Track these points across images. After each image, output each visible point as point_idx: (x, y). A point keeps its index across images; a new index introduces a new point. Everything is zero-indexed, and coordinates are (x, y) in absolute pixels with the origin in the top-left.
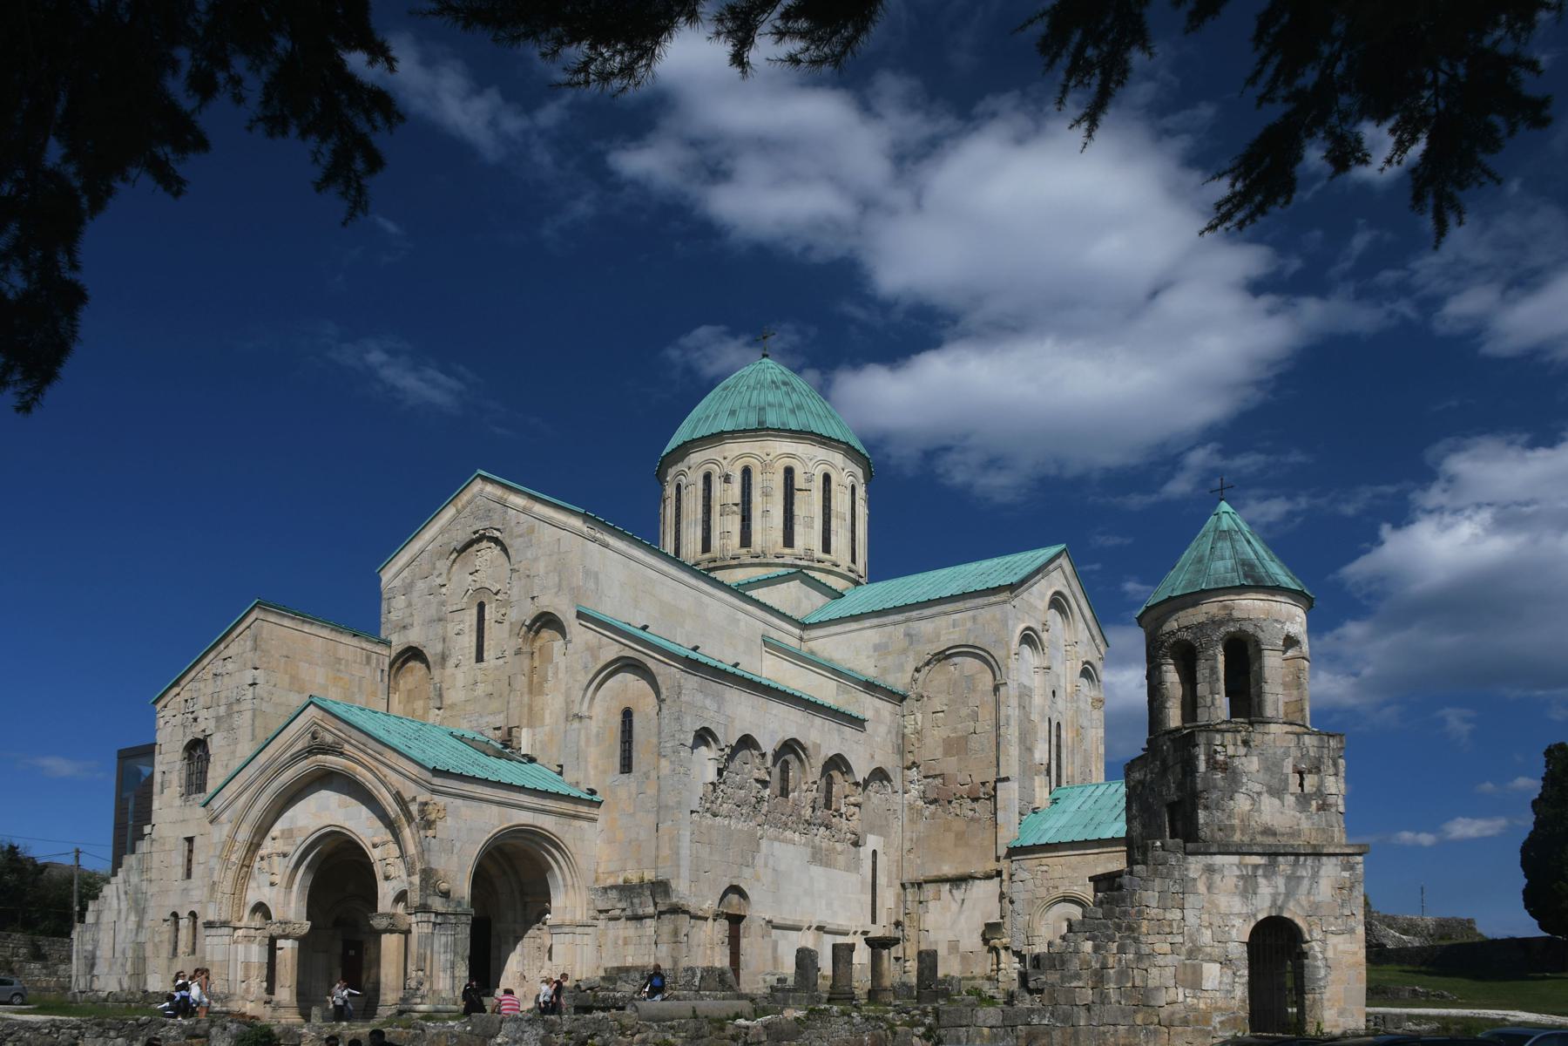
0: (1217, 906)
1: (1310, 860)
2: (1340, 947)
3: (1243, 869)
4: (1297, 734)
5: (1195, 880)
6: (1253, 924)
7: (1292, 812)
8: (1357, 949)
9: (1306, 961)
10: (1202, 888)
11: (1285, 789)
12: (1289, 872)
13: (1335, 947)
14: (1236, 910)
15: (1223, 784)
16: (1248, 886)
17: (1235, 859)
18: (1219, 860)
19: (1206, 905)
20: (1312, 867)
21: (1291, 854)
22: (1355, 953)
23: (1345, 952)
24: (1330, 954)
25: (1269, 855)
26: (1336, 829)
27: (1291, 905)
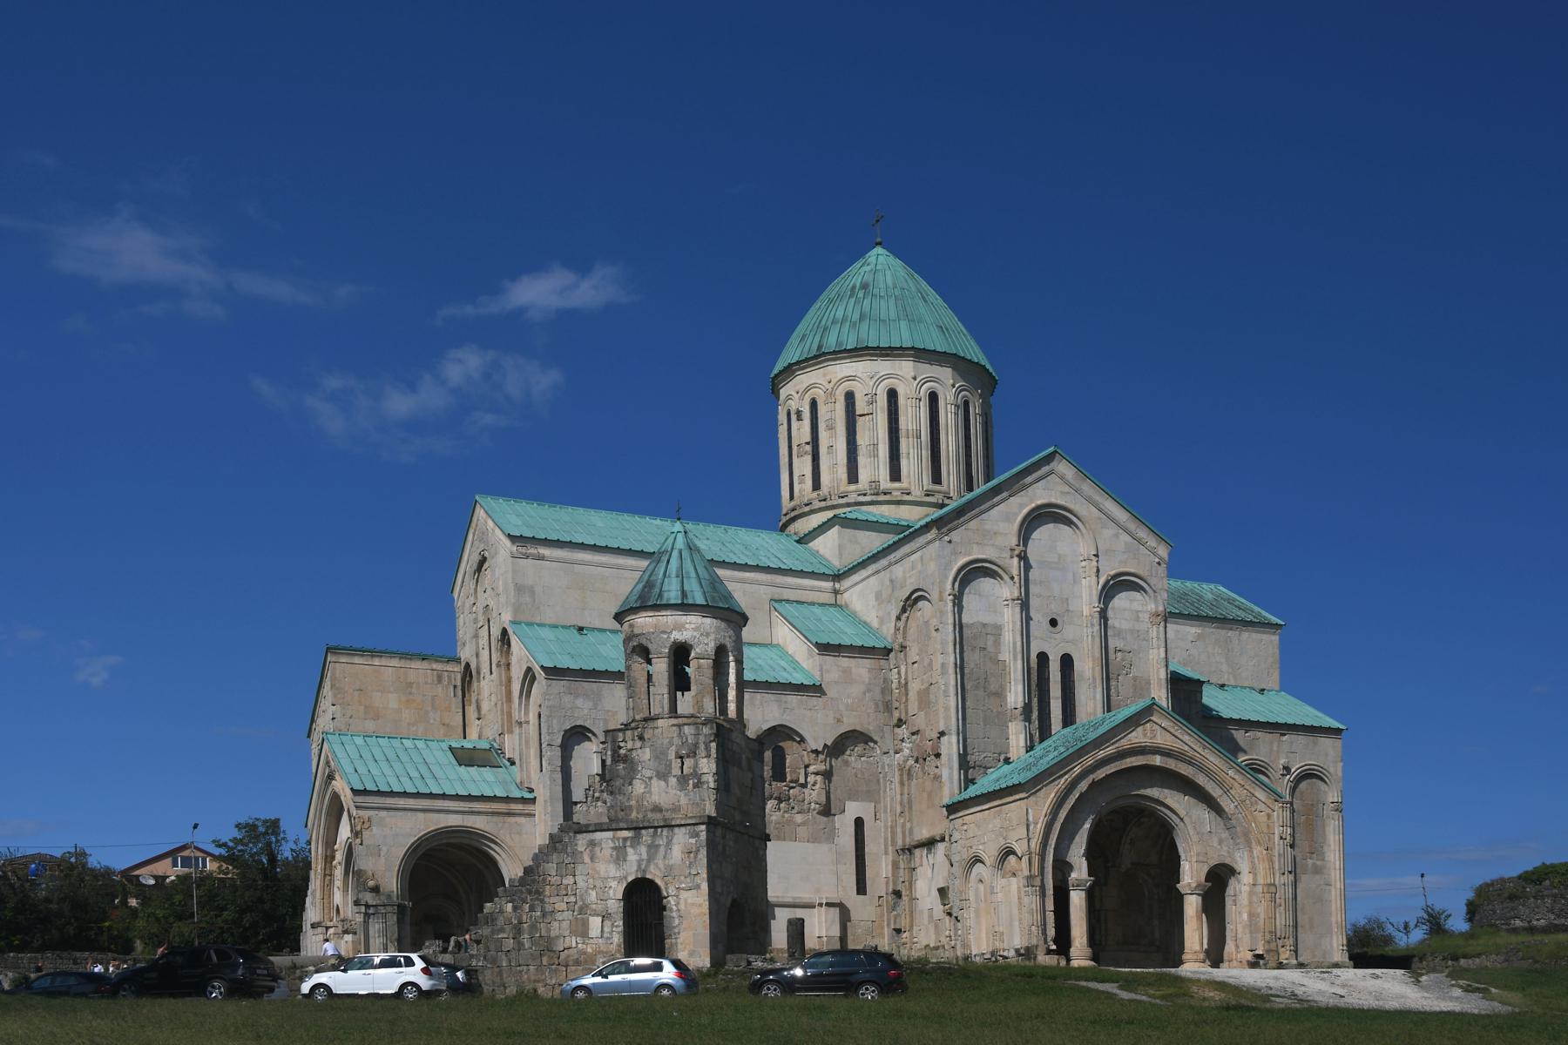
0: (598, 873)
1: (665, 830)
2: (689, 901)
3: (616, 842)
4: (679, 726)
5: (582, 852)
6: (625, 885)
7: (674, 792)
8: (702, 901)
9: (665, 913)
10: (587, 859)
11: (670, 772)
12: (649, 842)
13: (686, 900)
14: (611, 875)
15: (623, 773)
16: (620, 855)
17: (610, 834)
18: (598, 836)
19: (590, 872)
20: (667, 837)
21: (651, 827)
22: (700, 905)
23: (693, 904)
24: (682, 906)
25: (635, 829)
26: (707, 803)
27: (652, 868)
